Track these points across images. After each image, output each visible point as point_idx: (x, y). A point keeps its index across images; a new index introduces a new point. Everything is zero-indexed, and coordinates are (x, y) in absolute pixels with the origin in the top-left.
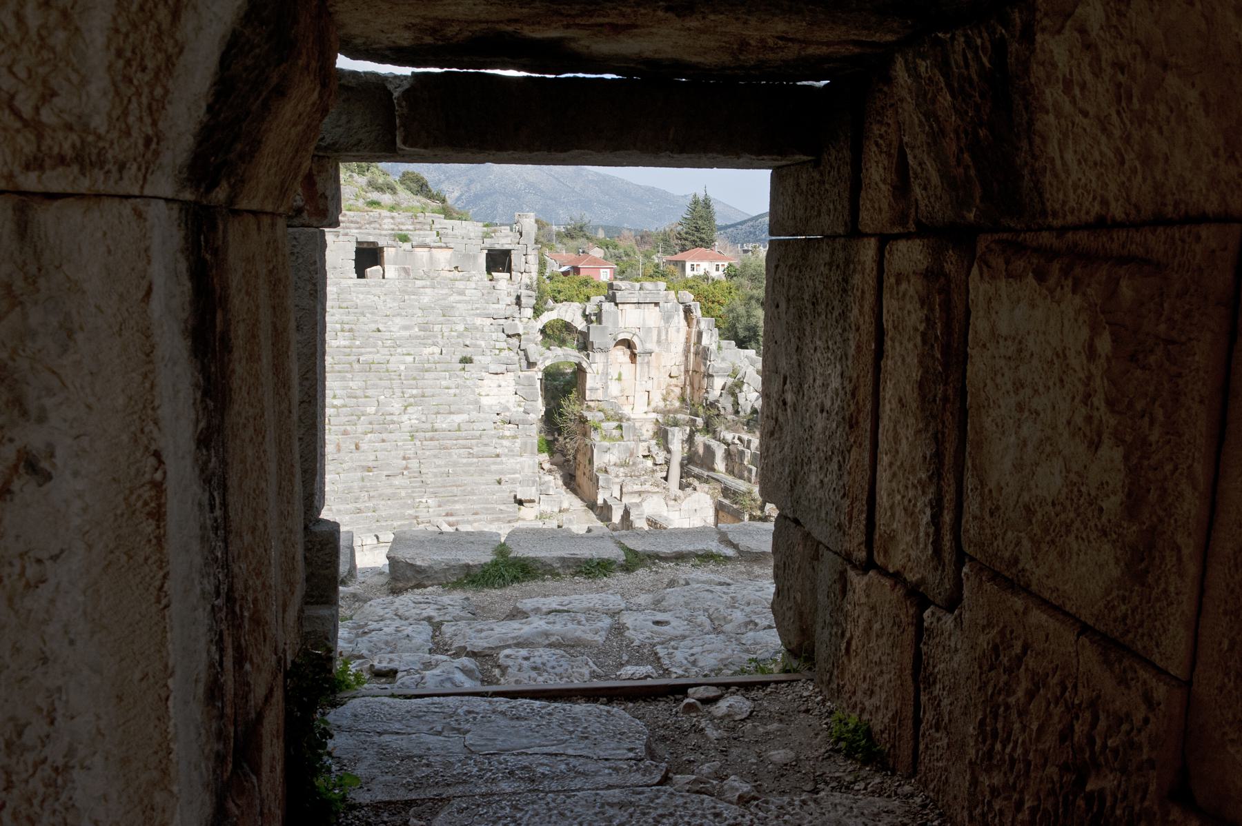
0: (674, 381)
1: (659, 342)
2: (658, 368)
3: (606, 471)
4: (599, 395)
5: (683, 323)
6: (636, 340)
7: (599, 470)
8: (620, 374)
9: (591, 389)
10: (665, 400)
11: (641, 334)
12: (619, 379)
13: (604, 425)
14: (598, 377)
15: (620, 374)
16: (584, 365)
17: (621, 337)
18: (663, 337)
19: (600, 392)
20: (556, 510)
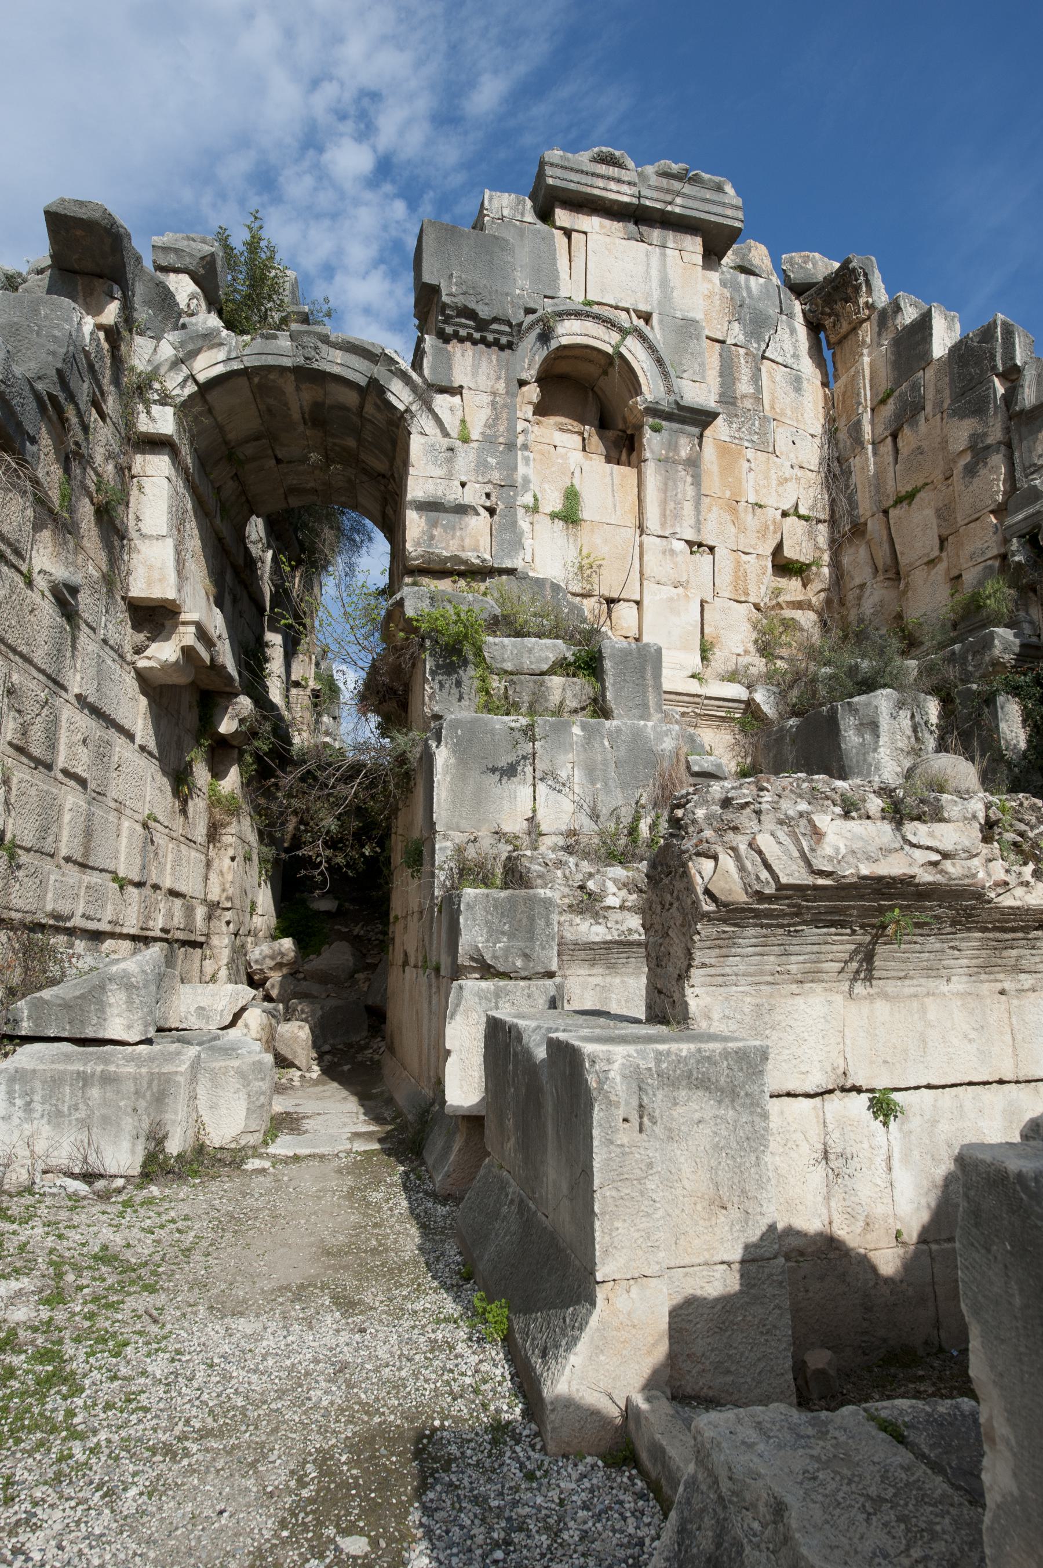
0: (792, 589)
1: (728, 398)
2: (733, 505)
3: (515, 875)
4: (474, 539)
5: (807, 367)
6: (636, 353)
7: (470, 872)
8: (572, 496)
9: (431, 507)
10: (765, 649)
11: (656, 333)
12: (569, 515)
13: (501, 647)
14: (466, 459)
15: (572, 496)
16: (400, 396)
17: (571, 332)
18: (744, 387)
19: (479, 524)
20: (122, 1157)
